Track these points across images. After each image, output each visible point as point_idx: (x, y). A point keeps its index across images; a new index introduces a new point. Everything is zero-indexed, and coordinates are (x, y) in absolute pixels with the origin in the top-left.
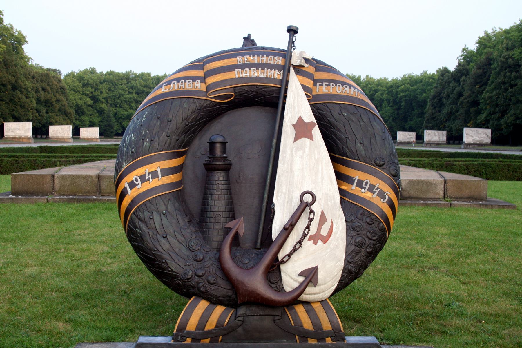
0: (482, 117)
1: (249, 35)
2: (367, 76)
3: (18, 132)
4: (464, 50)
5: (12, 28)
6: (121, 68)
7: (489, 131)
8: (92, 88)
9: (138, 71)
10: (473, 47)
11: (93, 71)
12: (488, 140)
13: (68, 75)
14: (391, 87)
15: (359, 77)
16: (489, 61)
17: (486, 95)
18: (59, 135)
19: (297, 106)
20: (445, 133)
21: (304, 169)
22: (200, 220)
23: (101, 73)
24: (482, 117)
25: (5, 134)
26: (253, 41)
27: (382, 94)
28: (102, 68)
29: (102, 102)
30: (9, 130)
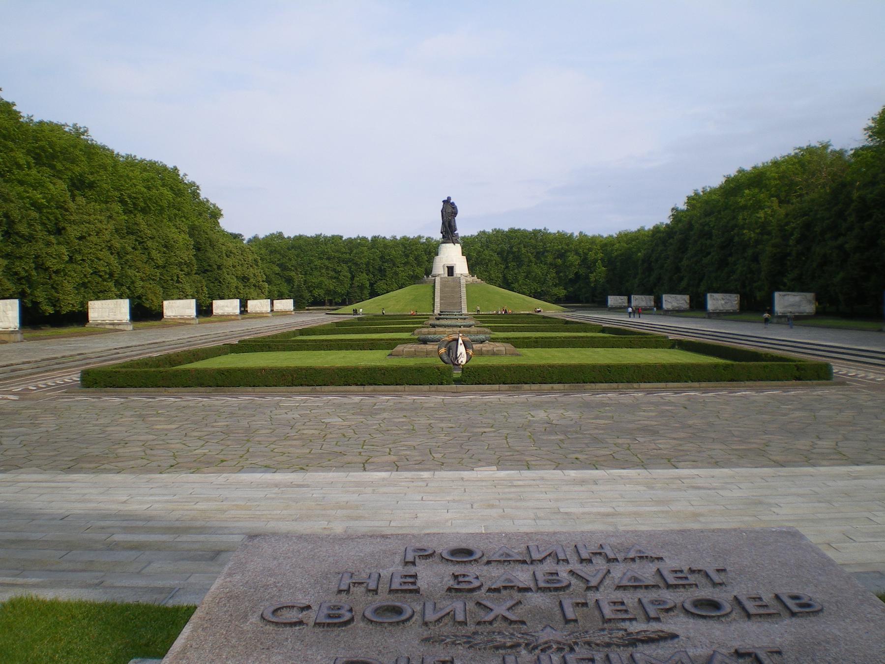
0: (684, 284)
1: (449, 198)
2: (581, 233)
3: (226, 309)
4: (673, 209)
5: (208, 201)
6: (310, 232)
7: (687, 297)
8: (280, 254)
9: (329, 233)
10: (682, 206)
11: (280, 235)
12: (686, 306)
13: (250, 241)
14: (606, 245)
15: (572, 234)
16: (690, 226)
17: (685, 262)
18: (258, 310)
19: (460, 341)
20: (652, 297)
21: (461, 349)
22: (449, 355)
23: (289, 238)
24: (684, 284)
25: (214, 311)
26: (453, 204)
27: (596, 253)
28: (290, 232)
29: (290, 270)
30: (218, 307)
